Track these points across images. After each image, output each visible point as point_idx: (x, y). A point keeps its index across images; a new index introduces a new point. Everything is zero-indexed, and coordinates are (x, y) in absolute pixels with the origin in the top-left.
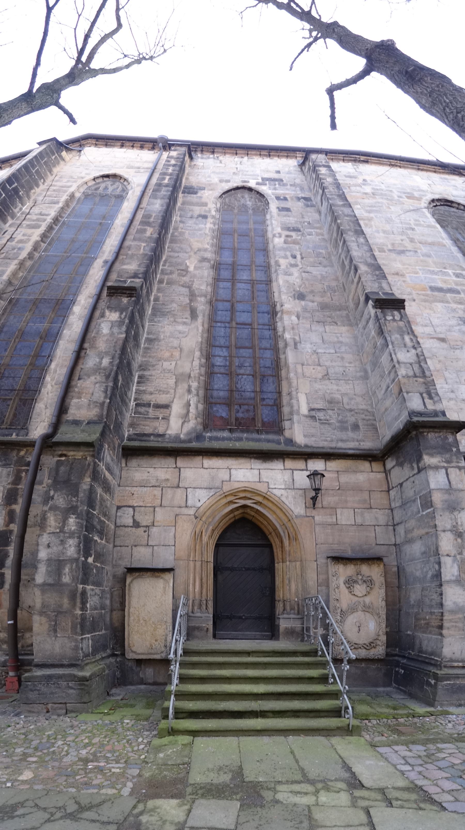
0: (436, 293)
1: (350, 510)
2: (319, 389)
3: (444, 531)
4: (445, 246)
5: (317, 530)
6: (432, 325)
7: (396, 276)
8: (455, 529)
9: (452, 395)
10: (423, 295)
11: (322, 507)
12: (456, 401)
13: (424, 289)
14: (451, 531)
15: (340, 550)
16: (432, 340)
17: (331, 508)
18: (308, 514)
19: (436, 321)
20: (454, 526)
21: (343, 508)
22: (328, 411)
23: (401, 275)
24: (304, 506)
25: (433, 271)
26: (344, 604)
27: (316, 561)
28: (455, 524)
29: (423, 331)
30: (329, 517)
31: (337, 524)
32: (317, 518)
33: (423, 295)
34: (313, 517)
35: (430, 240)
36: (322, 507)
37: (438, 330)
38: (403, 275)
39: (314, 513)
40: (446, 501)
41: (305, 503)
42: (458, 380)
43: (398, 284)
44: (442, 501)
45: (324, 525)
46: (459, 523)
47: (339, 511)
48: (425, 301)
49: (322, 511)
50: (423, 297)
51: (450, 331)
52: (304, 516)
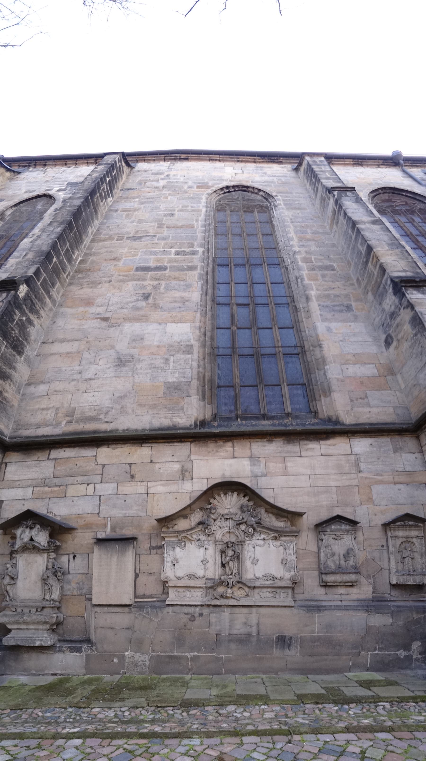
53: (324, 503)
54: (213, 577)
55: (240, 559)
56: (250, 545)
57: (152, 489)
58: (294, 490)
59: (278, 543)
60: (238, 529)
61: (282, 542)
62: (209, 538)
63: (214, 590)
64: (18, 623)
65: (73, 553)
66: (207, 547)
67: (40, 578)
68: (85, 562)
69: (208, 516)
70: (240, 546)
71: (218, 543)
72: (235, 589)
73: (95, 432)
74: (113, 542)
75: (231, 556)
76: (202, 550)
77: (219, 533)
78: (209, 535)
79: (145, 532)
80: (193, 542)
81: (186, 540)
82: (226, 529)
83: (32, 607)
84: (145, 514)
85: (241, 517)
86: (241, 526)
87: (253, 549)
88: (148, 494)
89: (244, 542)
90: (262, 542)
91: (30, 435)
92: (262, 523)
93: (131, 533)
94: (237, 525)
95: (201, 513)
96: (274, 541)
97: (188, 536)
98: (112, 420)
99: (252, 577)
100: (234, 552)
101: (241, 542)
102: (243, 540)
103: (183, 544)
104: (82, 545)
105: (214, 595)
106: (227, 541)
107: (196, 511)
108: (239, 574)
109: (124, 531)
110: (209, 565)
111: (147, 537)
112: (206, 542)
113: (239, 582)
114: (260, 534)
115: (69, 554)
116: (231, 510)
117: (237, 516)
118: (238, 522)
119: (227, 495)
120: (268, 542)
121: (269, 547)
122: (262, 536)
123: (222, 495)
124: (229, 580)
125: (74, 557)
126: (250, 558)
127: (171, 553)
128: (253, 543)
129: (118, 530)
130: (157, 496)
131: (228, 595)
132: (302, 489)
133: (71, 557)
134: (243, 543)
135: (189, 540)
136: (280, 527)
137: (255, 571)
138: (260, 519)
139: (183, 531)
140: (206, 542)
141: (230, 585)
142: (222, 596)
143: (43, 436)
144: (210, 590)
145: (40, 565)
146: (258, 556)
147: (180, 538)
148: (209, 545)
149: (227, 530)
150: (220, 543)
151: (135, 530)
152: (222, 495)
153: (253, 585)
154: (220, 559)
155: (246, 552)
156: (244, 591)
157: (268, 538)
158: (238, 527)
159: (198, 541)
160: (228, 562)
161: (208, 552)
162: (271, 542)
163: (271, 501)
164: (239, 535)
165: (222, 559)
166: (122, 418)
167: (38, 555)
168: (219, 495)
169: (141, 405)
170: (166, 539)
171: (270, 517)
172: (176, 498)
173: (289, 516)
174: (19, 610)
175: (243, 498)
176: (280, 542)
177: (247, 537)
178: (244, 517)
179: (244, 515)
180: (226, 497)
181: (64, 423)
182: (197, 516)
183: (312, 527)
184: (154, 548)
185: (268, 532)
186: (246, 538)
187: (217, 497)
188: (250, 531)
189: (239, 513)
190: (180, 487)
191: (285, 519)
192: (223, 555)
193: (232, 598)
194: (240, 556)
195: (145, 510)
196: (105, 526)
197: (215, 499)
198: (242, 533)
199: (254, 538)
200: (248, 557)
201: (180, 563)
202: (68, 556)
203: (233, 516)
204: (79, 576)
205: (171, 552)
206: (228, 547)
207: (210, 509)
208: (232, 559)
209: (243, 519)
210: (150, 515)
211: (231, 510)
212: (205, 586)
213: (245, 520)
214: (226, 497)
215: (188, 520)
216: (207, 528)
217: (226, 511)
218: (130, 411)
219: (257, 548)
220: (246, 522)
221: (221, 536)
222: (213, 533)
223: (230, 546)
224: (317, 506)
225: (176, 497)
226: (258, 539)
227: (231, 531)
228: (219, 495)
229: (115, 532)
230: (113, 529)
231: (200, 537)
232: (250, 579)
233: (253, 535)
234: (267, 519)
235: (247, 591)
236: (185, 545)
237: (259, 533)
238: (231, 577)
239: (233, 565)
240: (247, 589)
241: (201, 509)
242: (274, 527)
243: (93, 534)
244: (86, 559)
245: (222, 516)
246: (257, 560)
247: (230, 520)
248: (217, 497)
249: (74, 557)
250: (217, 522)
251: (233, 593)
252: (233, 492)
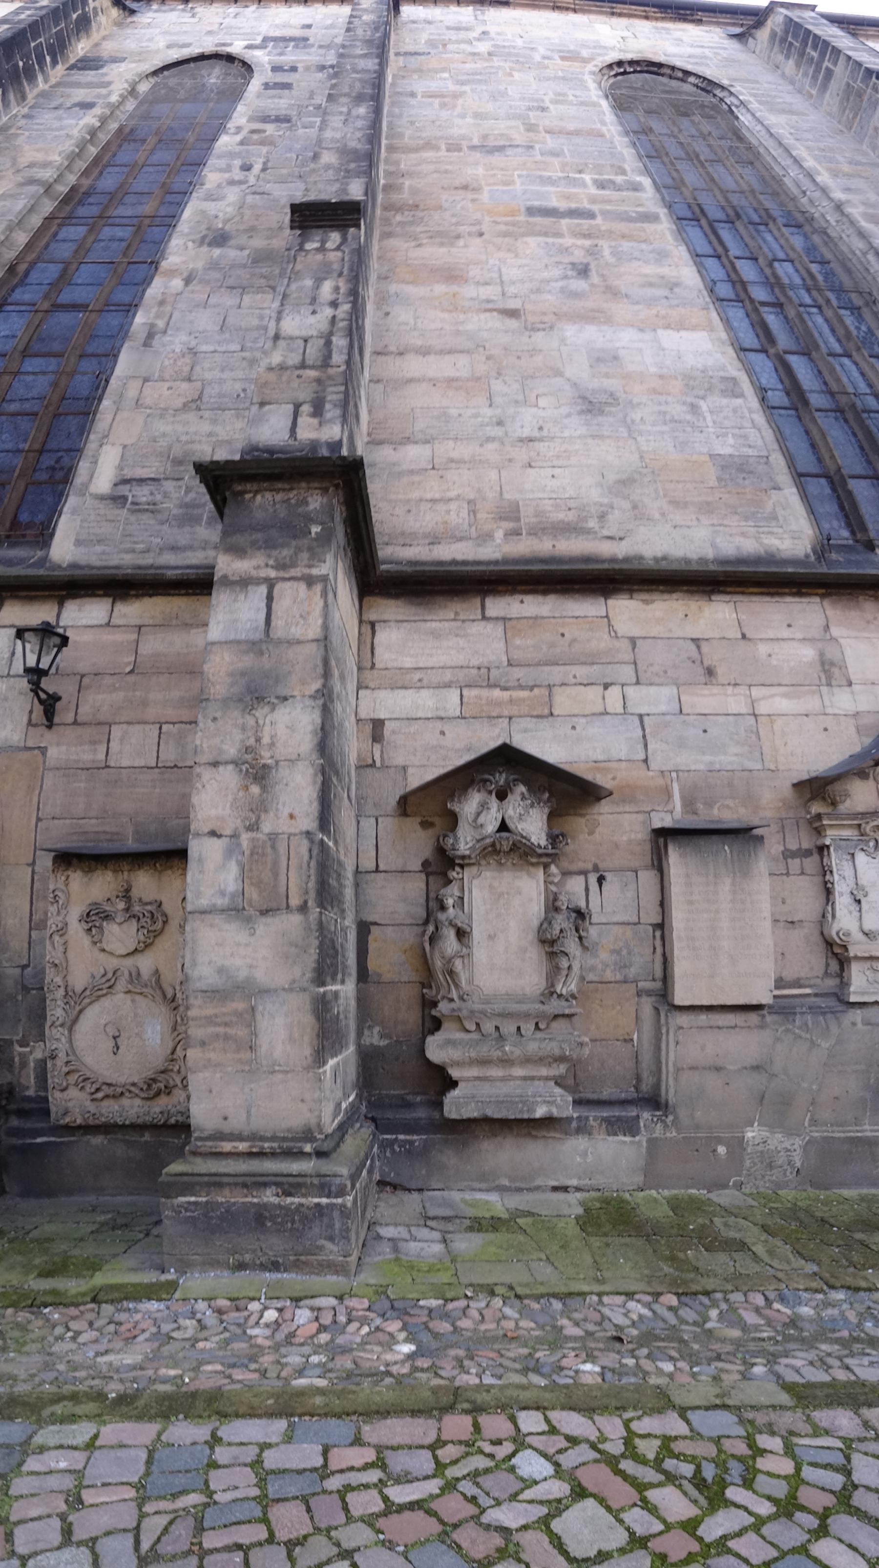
0: (538, 220)
1: (147, 727)
2: (164, 435)
3: (215, 764)
4: (602, 135)
5: (48, 783)
6: (502, 282)
7: (461, 192)
8: (248, 757)
9: (498, 431)
10: (506, 224)
11: (75, 723)
12: (503, 443)
13: (513, 213)
14: (235, 763)
15: (105, 832)
16: (488, 314)
17: (100, 724)
18: (30, 744)
19: (511, 273)
20: (248, 750)
21: (129, 723)
22: (165, 483)
23: (473, 190)
24: (25, 720)
25: (549, 178)
26: (79, 980)
27: (33, 863)
28: (252, 741)
29: (474, 295)
30: (86, 747)
31: (107, 767)
32: (53, 753)
33: (506, 224)
34: (43, 750)
35: (572, 126)
36: (75, 723)
37: (511, 290)
38: (477, 190)
39: (47, 738)
40: (243, 674)
41: (31, 712)
42: (521, 397)
43: (459, 206)
44: (231, 674)
45: (68, 770)
46: (266, 740)
47: (116, 732)
48: (505, 235)
49: (70, 732)
50: (503, 228)
51: (538, 291)
52: (19, 749)
64: (484, 1062)
65: (596, 868)
67: (532, 936)
68: (630, 893)
73: (587, 559)
74: (715, 838)
83: (527, 1016)
91: (418, 558)
93: (735, 816)
98: (622, 534)
104: (616, 846)
109: (715, 811)
115: (584, 873)
125: (601, 880)
129: (700, 806)
133: (593, 879)
143: (454, 562)
145: (531, 900)
151: (742, 811)
166: (642, 529)
167: (524, 874)
169: (675, 503)
174: (488, 1027)
181: (499, 535)
196: (669, 796)
202: (581, 879)
204: (615, 929)
218: (657, 516)
229: (695, 813)
230: (689, 804)
243: (641, 817)
244: (633, 886)
249: (601, 880)
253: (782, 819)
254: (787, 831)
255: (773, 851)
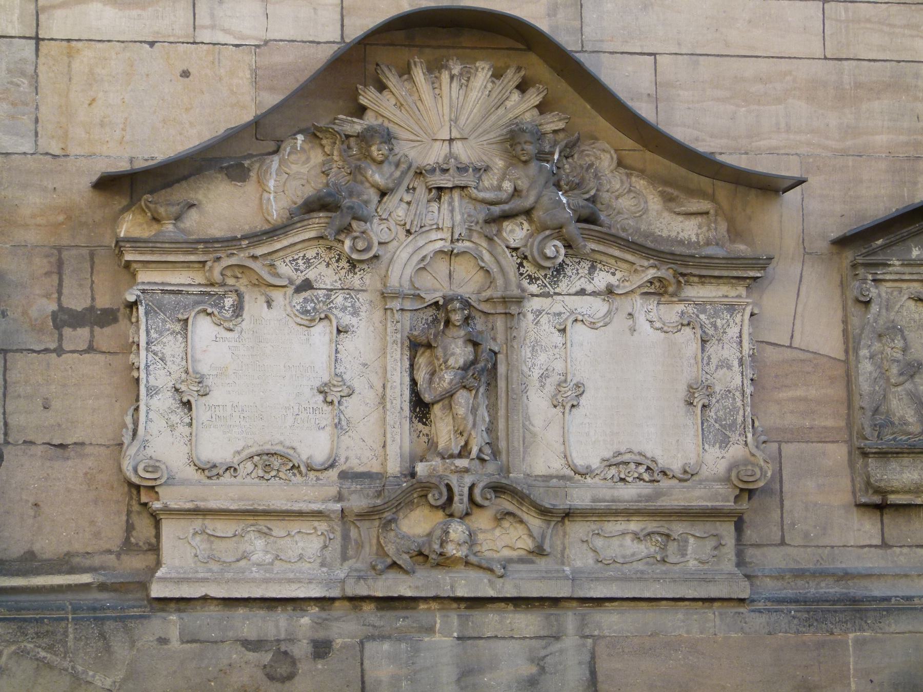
53: (881, 139)
54: (376, 468)
55: (502, 384)
56: (544, 319)
57: (59, 13)
58: (750, 68)
59: (672, 312)
60: (490, 239)
61: (691, 309)
62: (355, 280)
63: (387, 525)
66: (346, 319)
69: (356, 172)
70: (500, 323)
71: (396, 305)
72: (482, 520)
75: (465, 368)
76: (321, 334)
77: (403, 255)
78: (353, 265)
79: (32, 237)
80: (278, 296)
81: (242, 285)
82: (438, 241)
84: (28, 147)
85: (508, 186)
86: (508, 225)
87: (557, 338)
88: (38, 39)
89: (519, 301)
90: (598, 307)
92: (603, 217)
94: (487, 222)
95: (317, 157)
96: (652, 303)
97: (255, 265)
99: (556, 465)
100: (476, 345)
101: (505, 300)
102: (516, 292)
103: (229, 302)
105: (381, 551)
106: (437, 296)
107: (287, 148)
108: (496, 454)
110: (352, 407)
111: (41, 264)
112: (339, 299)
113: (498, 489)
114: (593, 268)
116: (458, 147)
117: (489, 181)
118: (496, 210)
119: (445, 76)
120: (626, 305)
121: (633, 330)
122: (602, 279)
123: (419, 74)
124: (454, 481)
126: (543, 377)
127: (171, 346)
128: (558, 308)
130: (87, 54)
131: (451, 550)
132: (784, 65)
134: (514, 309)
135: (260, 284)
136: (681, 243)
137: (572, 439)
138: (593, 200)
139: (230, 242)
140: (339, 299)
141: (459, 506)
142: (421, 555)
144: (364, 525)
146: (582, 371)
147: (217, 276)
148: (355, 313)
149: (438, 245)
150: (408, 305)
152: (419, 74)
153: (562, 504)
154: (407, 380)
155: (526, 352)
156: (520, 530)
157: (628, 287)
158: (494, 228)
159: (299, 289)
160: (449, 396)
161: (349, 344)
162: (639, 304)
163: (645, 110)
164: (494, 269)
165: (414, 382)
168: (405, 72)
170: (144, 276)
171: (638, 194)
172: (186, 74)
173: (723, 191)
175: (516, 96)
176: (680, 307)
177: (532, 279)
178: (523, 184)
179: (523, 177)
180: (435, 84)
182: (294, 168)
183: (822, 246)
184: (76, 319)
185: (629, 257)
186: (525, 283)
187: (392, 80)
188: (550, 251)
189: (499, 163)
190: (203, 18)
191: (705, 205)
192: (422, 360)
193: (467, 564)
194: (502, 369)
195: (27, 121)
197: (382, 87)
198: (511, 262)
199: (563, 286)
200: (536, 373)
201: (218, 396)
203: (468, 179)
205: (168, 339)
206: (448, 322)
207: (365, 138)
208: (471, 382)
209: (516, 192)
210: (55, 149)
211: (458, 147)
212: (338, 506)
213: (528, 202)
214: (435, 84)
215: (250, 187)
216: (347, 229)
217: (435, 154)
219: (579, 333)
220: (528, 213)
221: (409, 271)
222: (376, 257)
223: (456, 317)
224: (844, 153)
225: (181, 67)
226: (582, 292)
227: (461, 246)
228: (405, 72)
231: (311, 274)
232: (547, 478)
233: (560, 269)
234: (625, 203)
235: (536, 532)
236: (238, 309)
237: (586, 265)
238: (462, 463)
239: (474, 410)
240: (535, 522)
241: (314, 135)
242: (658, 239)
245: (419, 173)
246: (580, 389)
247: (456, 194)
248: (392, 80)
250: (391, 202)
251: (471, 539)
252: (468, 61)
253: (60, 249)
254: (67, 270)
255: (33, 312)
